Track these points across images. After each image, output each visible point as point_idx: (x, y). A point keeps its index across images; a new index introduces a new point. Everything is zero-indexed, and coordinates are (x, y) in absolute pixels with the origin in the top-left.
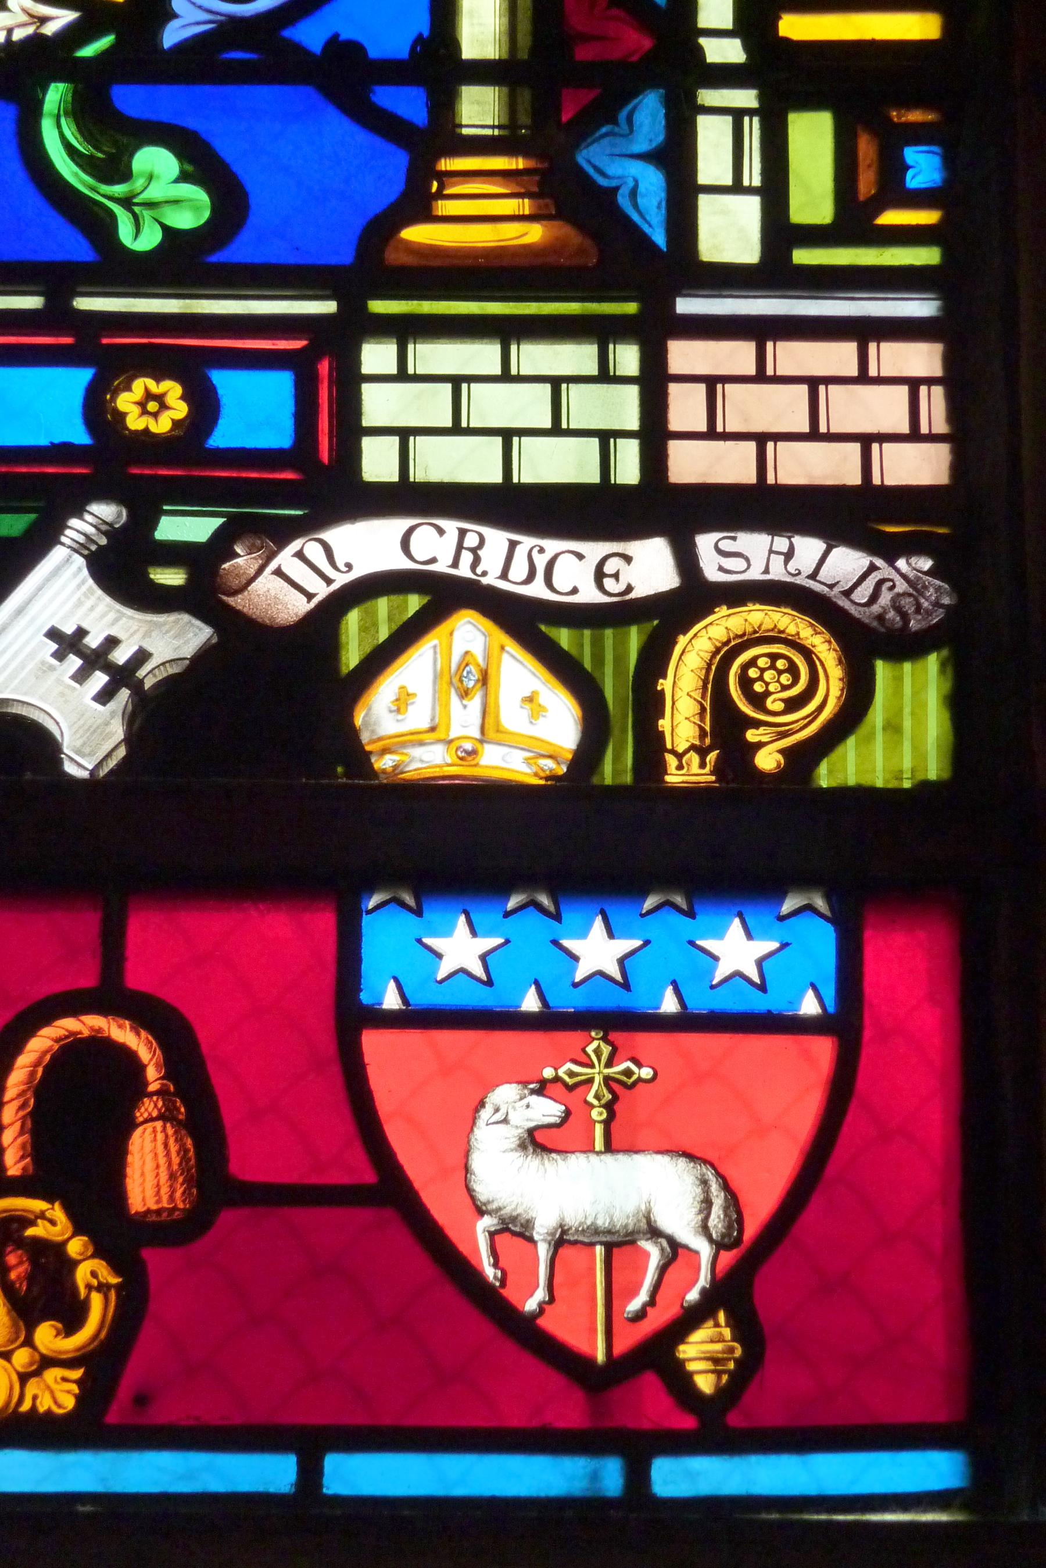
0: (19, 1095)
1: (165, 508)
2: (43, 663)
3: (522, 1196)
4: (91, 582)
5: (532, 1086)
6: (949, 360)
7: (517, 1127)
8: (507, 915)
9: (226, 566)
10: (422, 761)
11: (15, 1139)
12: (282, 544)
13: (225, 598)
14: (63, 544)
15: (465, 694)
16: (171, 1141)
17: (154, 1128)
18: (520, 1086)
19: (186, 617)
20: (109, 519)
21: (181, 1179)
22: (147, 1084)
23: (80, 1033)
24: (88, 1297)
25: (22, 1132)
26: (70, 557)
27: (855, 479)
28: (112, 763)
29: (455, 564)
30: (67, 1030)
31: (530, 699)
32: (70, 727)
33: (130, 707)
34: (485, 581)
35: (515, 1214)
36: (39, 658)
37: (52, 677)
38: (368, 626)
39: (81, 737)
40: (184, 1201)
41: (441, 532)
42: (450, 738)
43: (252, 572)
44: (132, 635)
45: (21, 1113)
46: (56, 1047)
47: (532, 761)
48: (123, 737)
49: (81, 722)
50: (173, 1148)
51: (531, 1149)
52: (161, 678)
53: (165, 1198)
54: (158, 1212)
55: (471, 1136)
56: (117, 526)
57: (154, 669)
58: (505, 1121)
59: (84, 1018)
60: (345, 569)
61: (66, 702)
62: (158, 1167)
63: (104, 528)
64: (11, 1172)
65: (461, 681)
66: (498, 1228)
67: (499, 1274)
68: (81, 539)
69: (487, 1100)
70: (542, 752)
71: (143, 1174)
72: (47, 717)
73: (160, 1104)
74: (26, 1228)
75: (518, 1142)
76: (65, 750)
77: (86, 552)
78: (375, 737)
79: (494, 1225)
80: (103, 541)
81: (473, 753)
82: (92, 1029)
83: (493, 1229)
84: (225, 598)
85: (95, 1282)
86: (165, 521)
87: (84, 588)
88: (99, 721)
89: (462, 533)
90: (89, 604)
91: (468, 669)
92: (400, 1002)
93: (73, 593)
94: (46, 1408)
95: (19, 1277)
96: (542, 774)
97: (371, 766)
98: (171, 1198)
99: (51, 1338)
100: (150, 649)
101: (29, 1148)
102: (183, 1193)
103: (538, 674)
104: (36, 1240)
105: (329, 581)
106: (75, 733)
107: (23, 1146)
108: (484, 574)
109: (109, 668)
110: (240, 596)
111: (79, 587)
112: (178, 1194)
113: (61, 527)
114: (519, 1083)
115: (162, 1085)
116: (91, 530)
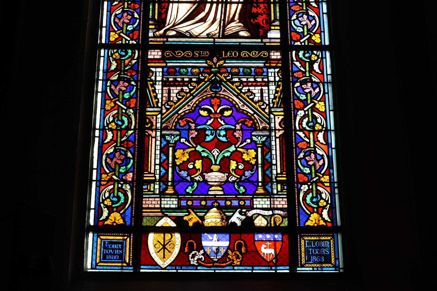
6: (287, 200)
27: (282, 207)
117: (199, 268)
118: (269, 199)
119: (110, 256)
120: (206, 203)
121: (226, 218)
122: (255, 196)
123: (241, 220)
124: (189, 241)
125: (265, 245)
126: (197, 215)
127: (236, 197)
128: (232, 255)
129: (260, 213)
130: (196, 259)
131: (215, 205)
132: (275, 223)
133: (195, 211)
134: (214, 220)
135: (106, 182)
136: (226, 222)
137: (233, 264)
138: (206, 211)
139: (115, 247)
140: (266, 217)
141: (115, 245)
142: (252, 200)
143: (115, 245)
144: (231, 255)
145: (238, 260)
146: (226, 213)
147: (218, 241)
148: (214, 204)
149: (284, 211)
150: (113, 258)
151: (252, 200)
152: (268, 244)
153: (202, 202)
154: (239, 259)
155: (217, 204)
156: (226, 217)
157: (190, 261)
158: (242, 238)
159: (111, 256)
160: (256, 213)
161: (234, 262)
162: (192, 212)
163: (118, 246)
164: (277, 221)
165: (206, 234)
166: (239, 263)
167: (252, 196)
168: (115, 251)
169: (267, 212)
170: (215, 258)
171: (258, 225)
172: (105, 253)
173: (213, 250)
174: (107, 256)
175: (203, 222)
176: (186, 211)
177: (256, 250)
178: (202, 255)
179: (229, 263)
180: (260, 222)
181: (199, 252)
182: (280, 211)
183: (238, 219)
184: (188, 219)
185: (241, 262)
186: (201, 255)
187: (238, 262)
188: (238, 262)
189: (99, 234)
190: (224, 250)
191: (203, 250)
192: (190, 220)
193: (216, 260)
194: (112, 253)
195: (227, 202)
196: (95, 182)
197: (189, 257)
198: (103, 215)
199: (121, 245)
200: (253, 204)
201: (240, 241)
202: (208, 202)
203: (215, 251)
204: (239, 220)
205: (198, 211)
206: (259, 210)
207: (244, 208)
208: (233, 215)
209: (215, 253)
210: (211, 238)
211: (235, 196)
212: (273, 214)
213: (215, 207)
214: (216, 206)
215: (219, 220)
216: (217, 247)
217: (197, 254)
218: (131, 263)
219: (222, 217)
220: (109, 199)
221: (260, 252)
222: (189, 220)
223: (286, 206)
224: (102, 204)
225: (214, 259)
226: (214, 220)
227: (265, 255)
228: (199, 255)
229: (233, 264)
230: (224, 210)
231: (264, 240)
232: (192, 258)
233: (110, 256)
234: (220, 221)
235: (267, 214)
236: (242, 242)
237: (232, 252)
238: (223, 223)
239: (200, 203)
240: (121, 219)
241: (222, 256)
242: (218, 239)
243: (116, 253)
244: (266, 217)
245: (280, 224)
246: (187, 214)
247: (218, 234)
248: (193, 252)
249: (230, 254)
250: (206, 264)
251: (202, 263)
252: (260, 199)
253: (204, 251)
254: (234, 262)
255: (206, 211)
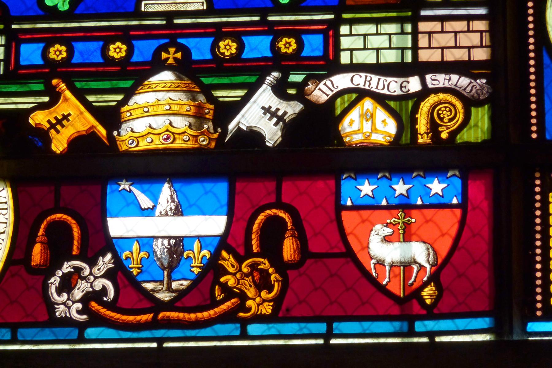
0: (256, 231)
1: (291, 73)
2: (261, 116)
3: (382, 254)
4: (272, 93)
5: (384, 225)
6: (490, 25)
7: (381, 236)
8: (378, 179)
9: (306, 88)
10: (356, 139)
11: (255, 242)
12: (320, 82)
13: (306, 97)
14: (265, 84)
15: (367, 120)
16: (294, 242)
17: (290, 239)
18: (381, 225)
19: (296, 102)
20: (277, 76)
21: (297, 252)
22: (288, 227)
23: (271, 214)
24: (274, 283)
25: (257, 241)
26: (267, 87)
27: (466, 58)
28: (278, 142)
29: (364, 85)
30: (268, 214)
31: (384, 121)
32: (267, 133)
33: (282, 127)
34: (372, 89)
35: (380, 259)
36: (259, 115)
37: (264, 119)
38: (343, 103)
39: (270, 135)
40: (297, 258)
41: (361, 77)
42: (363, 132)
43: (313, 89)
44: (283, 108)
45: (257, 236)
46: (265, 218)
47: (384, 138)
48: (281, 135)
49: (270, 132)
50: (295, 244)
51: (384, 242)
52: (290, 119)
53: (293, 257)
54: (291, 261)
55: (369, 239)
56: (279, 78)
57: (288, 117)
58: (378, 234)
59: (272, 210)
60: (336, 88)
61: (266, 126)
62: (291, 249)
63: (276, 79)
64: (254, 251)
65: (366, 117)
66: (376, 262)
67: (377, 275)
68: (270, 82)
69: (373, 229)
70: (387, 135)
71: (287, 251)
72: (262, 130)
73: (291, 232)
74: (258, 266)
75: (381, 240)
76: (266, 139)
77: (271, 86)
78: (344, 133)
79: (375, 262)
80: (275, 83)
81: (369, 136)
82: (274, 213)
83: (375, 263)
84: (306, 97)
85: (276, 280)
86: (291, 76)
87: (271, 95)
88: (275, 131)
89: (366, 77)
90: (272, 99)
91: (368, 113)
92: (351, 203)
93: (268, 97)
94: (264, 313)
95: (257, 279)
96: (387, 141)
97: (343, 140)
98: (294, 257)
99: (265, 294)
100: (287, 111)
101: (259, 245)
102: (297, 256)
103: (385, 114)
104: (261, 269)
105: (332, 91)
106: (269, 134)
107: (257, 245)
108: (372, 88)
109: (277, 116)
110: (310, 96)
111: (269, 95)
112: (296, 256)
113: (265, 79)
114: (381, 224)
115: (292, 227)
116: (272, 80)
117: (91, 332)
118: (409, 28)
120: (130, 51)
121: (214, 115)
122: (345, 16)
123: (280, 119)
124: (49, 218)
125: (387, 225)
126: (88, 106)
127: (263, 22)
128: (238, 276)
129: (367, 87)
130: (78, 294)
131: (167, 59)
132: (434, 127)
133: (78, 85)
134: (160, 123)
136: (216, 131)
137: (241, 314)
138: (128, 84)
140: (392, 104)
142: (331, 33)
144: (234, 275)
145: (264, 294)
146: (218, 93)
147: (178, 212)
148: (164, 55)
149: (475, 77)
151: (331, 33)
152: (401, 221)
153: (112, 47)
154: (270, 290)
155: (179, 55)
156: (215, 110)
157: (51, 306)
158: (285, 199)
160: (350, 85)
161: (249, 303)
162: (68, 94)
164: (441, 119)
165: (125, 185)
166: (267, 309)
167: (332, 17)
169: (400, 80)
170: (165, 286)
171: (357, 138)
173: (155, 252)
175: (115, 133)
176: (40, 87)
177: (344, 250)
178: (108, 275)
179: (224, 307)
180: (367, 127)
181: (92, 263)
182: (455, 77)
183: (268, 115)
184: (49, 121)
185: (277, 302)
186: (102, 277)
187: (264, 301)
188: (264, 301)
190: (205, 253)
191: (109, 256)
192: (58, 127)
193: (165, 296)
195: (222, 44)
197: (46, 287)
200: (338, 50)
201: (275, 211)
202: (138, 44)
203: (166, 258)
204: (275, 120)
205: (94, 85)
206: (363, 75)
207: (298, 69)
208: (245, 100)
209: (163, 268)
210: (145, 202)
211: (256, 18)
212: (425, 92)
213: (170, 68)
214: (170, 61)
215: (181, 123)
216: (173, 241)
217: (87, 272)
219: (200, 107)
221: (361, 257)
222: (53, 126)
223: (481, 55)
225: (158, 291)
226: (160, 123)
227: (388, 268)
228: (92, 278)
229: (241, 314)
230: (206, 81)
231: (384, 203)
232: (59, 292)
234: (190, 126)
235: (398, 92)
236: (282, 214)
237: (240, 260)
238: (202, 134)
239: (104, 51)
241: (193, 277)
242: (177, 207)
244: (392, 104)
245: (453, 134)
246: (46, 99)
247: (177, 186)
248: (67, 268)
249: (231, 270)
250: (124, 314)
251: (103, 310)
252: (370, 28)
253: (117, 258)
254: (249, 303)
255: (128, 84)
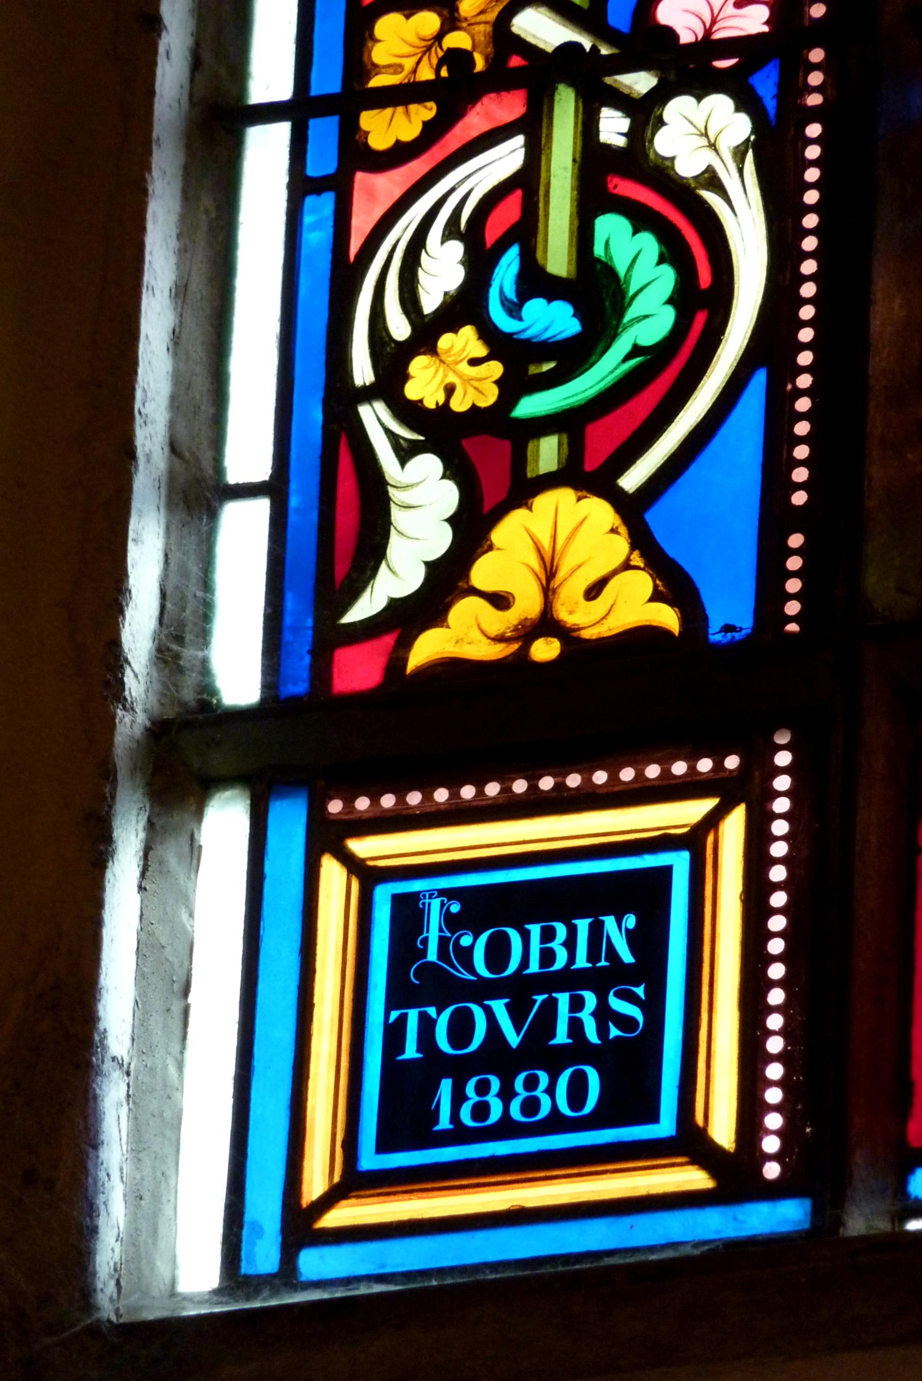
119: (484, 1088)
135: (426, 112)
139: (548, 957)
141: (548, 935)
143: (548, 935)
150: (531, 1106)
159: (495, 1084)
163: (596, 931)
168: (551, 1007)
172: (411, 1051)
174: (446, 1087)
189: (335, 807)
194: (513, 1039)
196: (282, 130)
198: (396, 547)
199: (630, 921)
218: (771, 1144)
220: (468, 332)
224: (380, 407)
233: (484, 1088)
240: (627, 566)
243: (562, 1036)
